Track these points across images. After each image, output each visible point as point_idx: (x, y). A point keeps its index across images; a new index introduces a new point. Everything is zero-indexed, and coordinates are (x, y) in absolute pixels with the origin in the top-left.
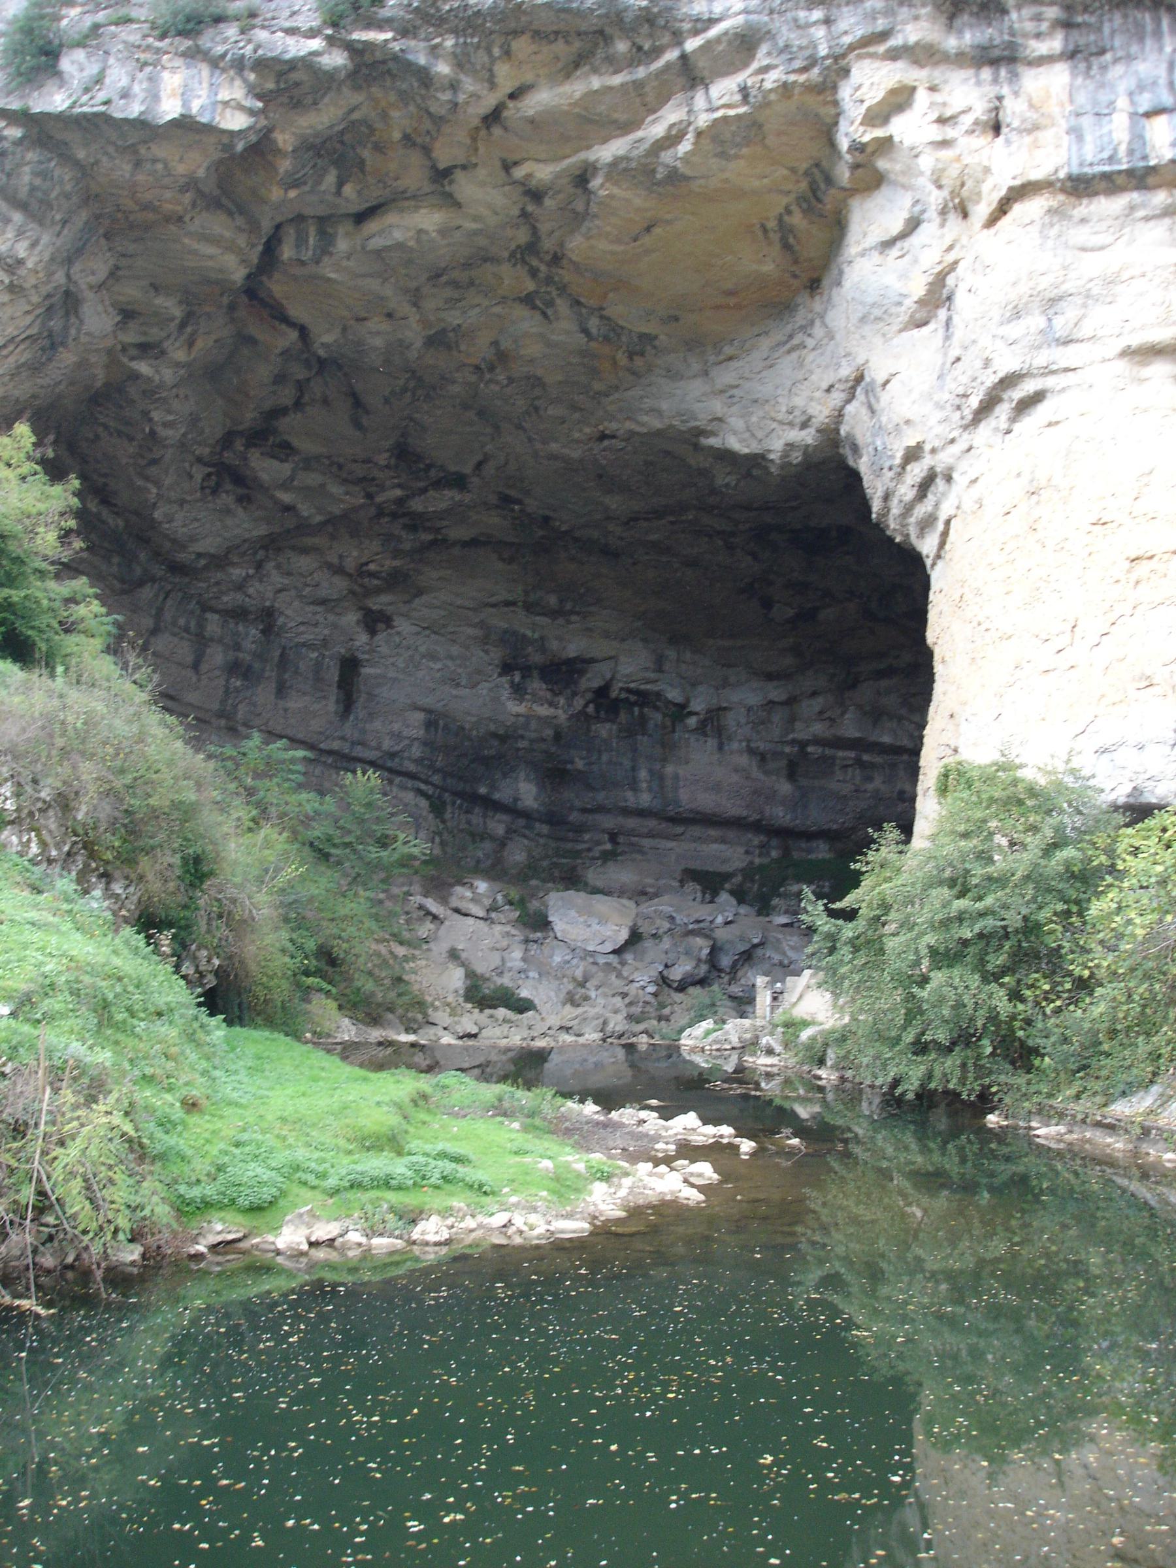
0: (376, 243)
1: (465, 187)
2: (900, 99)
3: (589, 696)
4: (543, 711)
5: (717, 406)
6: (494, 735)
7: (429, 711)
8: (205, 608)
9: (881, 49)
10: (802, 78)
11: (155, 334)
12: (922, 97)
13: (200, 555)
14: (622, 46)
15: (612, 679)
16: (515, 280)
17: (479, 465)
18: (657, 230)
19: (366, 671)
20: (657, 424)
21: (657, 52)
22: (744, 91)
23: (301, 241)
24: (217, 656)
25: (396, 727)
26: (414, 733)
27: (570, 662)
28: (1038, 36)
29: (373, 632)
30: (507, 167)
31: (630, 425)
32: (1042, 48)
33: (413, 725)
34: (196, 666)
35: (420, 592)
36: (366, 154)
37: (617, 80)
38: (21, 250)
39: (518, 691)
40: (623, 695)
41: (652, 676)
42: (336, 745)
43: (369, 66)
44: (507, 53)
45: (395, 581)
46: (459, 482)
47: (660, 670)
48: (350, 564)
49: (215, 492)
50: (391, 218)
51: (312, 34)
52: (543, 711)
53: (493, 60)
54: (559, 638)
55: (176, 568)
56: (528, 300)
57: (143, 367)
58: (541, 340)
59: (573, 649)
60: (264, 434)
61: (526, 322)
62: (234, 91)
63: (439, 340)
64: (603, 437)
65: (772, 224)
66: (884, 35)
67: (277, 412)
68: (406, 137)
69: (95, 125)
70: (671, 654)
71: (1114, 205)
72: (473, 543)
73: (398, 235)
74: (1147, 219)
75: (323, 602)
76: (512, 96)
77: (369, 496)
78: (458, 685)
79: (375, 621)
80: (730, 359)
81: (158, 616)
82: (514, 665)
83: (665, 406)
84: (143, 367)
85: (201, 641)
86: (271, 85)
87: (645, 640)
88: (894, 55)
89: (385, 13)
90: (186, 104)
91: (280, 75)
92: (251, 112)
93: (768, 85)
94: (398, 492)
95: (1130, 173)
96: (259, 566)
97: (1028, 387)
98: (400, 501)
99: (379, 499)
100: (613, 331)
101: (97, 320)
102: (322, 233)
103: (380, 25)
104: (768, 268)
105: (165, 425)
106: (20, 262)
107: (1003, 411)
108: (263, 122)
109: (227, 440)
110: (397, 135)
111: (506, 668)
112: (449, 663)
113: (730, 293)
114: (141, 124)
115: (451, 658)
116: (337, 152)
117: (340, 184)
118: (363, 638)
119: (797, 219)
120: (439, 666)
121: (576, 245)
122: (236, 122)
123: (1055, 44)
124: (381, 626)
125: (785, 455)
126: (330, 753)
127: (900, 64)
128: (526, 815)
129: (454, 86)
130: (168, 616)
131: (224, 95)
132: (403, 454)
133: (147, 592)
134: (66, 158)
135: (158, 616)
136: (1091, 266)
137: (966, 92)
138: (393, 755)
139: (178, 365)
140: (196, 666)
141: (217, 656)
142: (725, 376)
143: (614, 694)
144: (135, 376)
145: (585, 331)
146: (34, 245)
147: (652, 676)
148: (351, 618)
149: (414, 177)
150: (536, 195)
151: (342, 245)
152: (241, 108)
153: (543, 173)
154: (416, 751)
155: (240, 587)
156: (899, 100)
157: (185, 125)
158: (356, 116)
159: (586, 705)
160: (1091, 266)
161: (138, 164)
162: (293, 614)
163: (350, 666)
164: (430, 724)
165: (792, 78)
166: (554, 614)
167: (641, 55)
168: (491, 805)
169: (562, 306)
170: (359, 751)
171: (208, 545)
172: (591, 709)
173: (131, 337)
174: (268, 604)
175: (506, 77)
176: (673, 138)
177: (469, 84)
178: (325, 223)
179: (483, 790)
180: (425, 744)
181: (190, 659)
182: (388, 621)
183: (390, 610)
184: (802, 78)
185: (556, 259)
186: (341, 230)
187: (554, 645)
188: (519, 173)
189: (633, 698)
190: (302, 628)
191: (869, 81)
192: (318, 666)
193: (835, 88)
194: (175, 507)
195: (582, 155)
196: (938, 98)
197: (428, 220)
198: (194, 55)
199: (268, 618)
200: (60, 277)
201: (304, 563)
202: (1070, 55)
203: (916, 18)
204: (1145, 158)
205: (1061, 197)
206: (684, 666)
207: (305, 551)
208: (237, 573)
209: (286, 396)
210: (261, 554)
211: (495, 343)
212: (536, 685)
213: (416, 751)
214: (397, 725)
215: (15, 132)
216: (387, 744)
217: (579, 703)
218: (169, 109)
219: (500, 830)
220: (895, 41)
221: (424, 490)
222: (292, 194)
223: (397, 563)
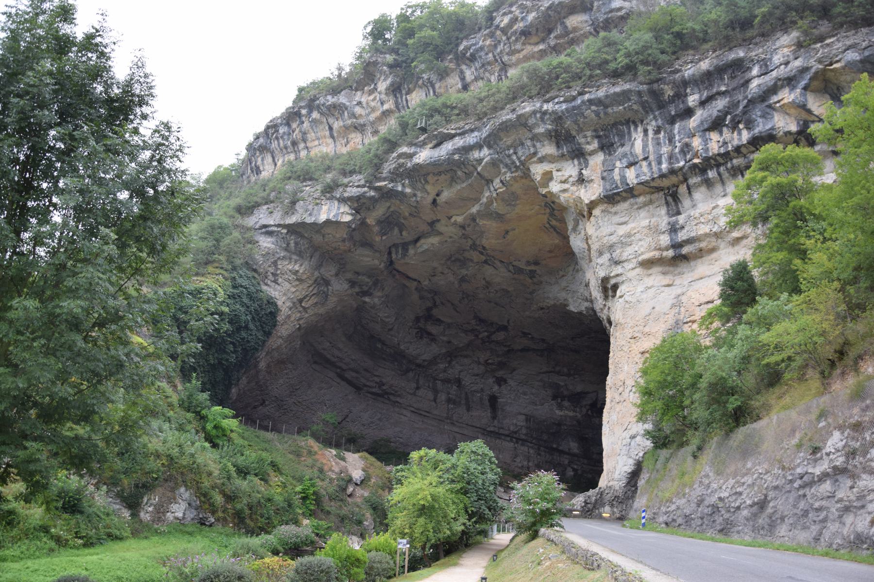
0: (420, 250)
1: (440, 227)
2: (549, 176)
3: (588, 407)
4: (571, 414)
5: (563, 295)
8: (435, 379)
9: (535, 159)
10: (517, 174)
11: (365, 288)
12: (555, 174)
13: (424, 361)
14: (459, 173)
15: (597, 399)
16: (475, 256)
17: (508, 321)
18: (510, 233)
20: (552, 303)
21: (472, 173)
22: (501, 181)
23: (397, 253)
24: (443, 397)
25: (515, 421)
26: (522, 424)
27: (578, 394)
28: (588, 143)
29: (500, 385)
30: (450, 218)
31: (545, 304)
32: (590, 148)
33: (521, 421)
34: (435, 400)
35: (514, 370)
36: (403, 221)
37: (464, 185)
38: (297, 268)
39: (560, 407)
42: (492, 429)
43: (387, 195)
44: (427, 182)
45: (502, 365)
46: (504, 328)
48: (481, 360)
49: (421, 338)
50: (422, 241)
51: (364, 186)
52: (571, 414)
53: (424, 185)
55: (419, 366)
56: (486, 262)
57: (367, 299)
58: (499, 276)
59: (579, 388)
60: (429, 316)
61: (489, 271)
62: (345, 209)
63: (463, 280)
64: (542, 309)
65: (547, 226)
66: (535, 154)
67: (429, 309)
68: (410, 214)
69: (303, 224)
71: (625, 205)
72: (522, 350)
73: (425, 247)
74: (640, 208)
75: (477, 375)
76: (438, 195)
77: (477, 336)
78: (536, 405)
79: (500, 381)
80: (563, 276)
81: (418, 382)
82: (558, 396)
83: (551, 296)
84: (367, 299)
85: (436, 392)
86: (356, 205)
88: (541, 160)
89: (384, 175)
90: (328, 214)
91: (357, 201)
92: (352, 214)
93: (508, 179)
94: (486, 334)
95: (625, 191)
96: (450, 362)
97: (613, 282)
98: (488, 337)
99: (480, 336)
100: (520, 271)
101: (339, 286)
102: (403, 248)
103: (384, 179)
104: (557, 241)
105: (386, 317)
106: (297, 271)
107: (610, 293)
108: (359, 217)
109: (418, 319)
110: (407, 214)
111: (555, 398)
113: (550, 252)
114: (315, 224)
115: (533, 394)
116: (389, 223)
117: (401, 232)
118: (496, 388)
119: (554, 223)
121: (484, 242)
122: (347, 218)
123: (595, 145)
124: (502, 383)
125: (587, 312)
126: (491, 432)
127: (544, 164)
128: (574, 455)
129: (415, 195)
130: (421, 382)
131: (342, 210)
132: (482, 321)
133: (411, 374)
134: (302, 236)
135: (418, 382)
136: (622, 230)
137: (570, 170)
138: (516, 433)
139: (379, 297)
140: (435, 400)
141: (443, 397)
142: (564, 284)
144: (365, 302)
145: (510, 271)
146: (301, 265)
148: (491, 380)
149: (425, 228)
150: (463, 227)
151: (411, 252)
152: (348, 214)
153: (460, 219)
154: (524, 431)
155: (445, 371)
156: (548, 177)
157: (328, 222)
158: (392, 209)
159: (587, 411)
160: (622, 230)
161: (323, 236)
162: (467, 380)
163: (493, 400)
165: (513, 175)
166: (569, 375)
167: (468, 175)
168: (562, 452)
169: (498, 263)
170: (501, 431)
171: (426, 357)
172: (589, 412)
173: (357, 289)
175: (432, 190)
176: (490, 201)
177: (419, 194)
178: (405, 246)
179: (555, 446)
180: (527, 428)
181: (432, 398)
182: (505, 381)
183: (505, 376)
184: (517, 174)
185: (484, 248)
186: (410, 247)
187: (571, 387)
188: (453, 220)
191: (538, 170)
192: (481, 399)
193: (529, 176)
195: (469, 212)
196: (560, 173)
197: (434, 240)
198: (332, 198)
199: (458, 382)
200: (316, 274)
201: (466, 361)
202: (602, 148)
203: (543, 146)
204: (628, 185)
205: (606, 205)
207: (466, 356)
208: (442, 366)
209: (429, 304)
210: (449, 359)
211: (484, 279)
212: (566, 403)
213: (524, 431)
214: (514, 421)
215: (285, 231)
216: (512, 428)
217: (584, 410)
218: (323, 218)
219: (566, 462)
220: (540, 155)
221: (495, 332)
222: (384, 238)
223: (500, 359)
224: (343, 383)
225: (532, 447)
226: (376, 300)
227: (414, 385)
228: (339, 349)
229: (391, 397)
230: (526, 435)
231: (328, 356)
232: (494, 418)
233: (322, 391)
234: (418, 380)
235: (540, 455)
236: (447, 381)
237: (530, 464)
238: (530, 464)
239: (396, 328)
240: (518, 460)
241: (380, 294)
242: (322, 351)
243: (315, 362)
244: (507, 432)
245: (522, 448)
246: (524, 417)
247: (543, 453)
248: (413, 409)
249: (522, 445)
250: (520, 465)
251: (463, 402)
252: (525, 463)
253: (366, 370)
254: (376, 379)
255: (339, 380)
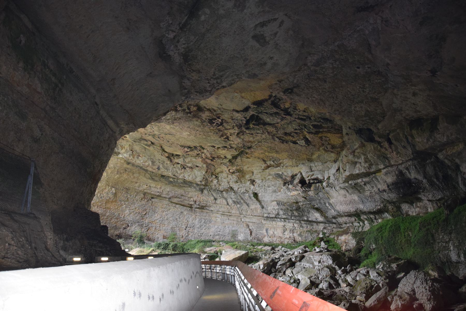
6: (294, 202)
7: (276, 201)
8: (222, 192)
19: (259, 195)
40: (312, 181)
41: (311, 173)
47: (312, 171)
54: (285, 171)
70: (312, 165)
87: (303, 164)
111: (285, 184)
112: (272, 187)
115: (273, 185)
120: (271, 189)
130: (214, 195)
133: (205, 192)
140: (228, 204)
143: (307, 182)
147: (311, 173)
162: (235, 187)
164: (278, 204)
170: (271, 216)
174: (228, 186)
179: (306, 219)
181: (226, 203)
189: (316, 181)
190: (240, 189)
194: (183, 175)
206: (318, 167)
224: (177, 206)
225: (295, 223)
226: (125, 155)
227: (212, 198)
228: (155, 187)
229: (207, 208)
230: (284, 214)
231: (152, 193)
232: (263, 207)
233: (164, 213)
234: (212, 194)
235: (303, 227)
236: (227, 191)
237: (295, 235)
238: (295, 235)
239: (161, 166)
240: (286, 233)
241: (123, 151)
242: (145, 191)
243: (152, 198)
244: (273, 216)
245: (289, 224)
246: (275, 202)
247: (305, 225)
248: (221, 213)
249: (289, 222)
250: (288, 237)
251: (242, 202)
252: (291, 235)
253: (182, 195)
254: (192, 199)
255: (174, 205)
